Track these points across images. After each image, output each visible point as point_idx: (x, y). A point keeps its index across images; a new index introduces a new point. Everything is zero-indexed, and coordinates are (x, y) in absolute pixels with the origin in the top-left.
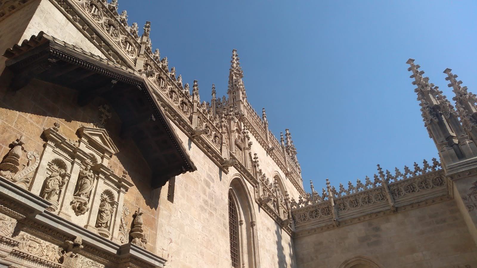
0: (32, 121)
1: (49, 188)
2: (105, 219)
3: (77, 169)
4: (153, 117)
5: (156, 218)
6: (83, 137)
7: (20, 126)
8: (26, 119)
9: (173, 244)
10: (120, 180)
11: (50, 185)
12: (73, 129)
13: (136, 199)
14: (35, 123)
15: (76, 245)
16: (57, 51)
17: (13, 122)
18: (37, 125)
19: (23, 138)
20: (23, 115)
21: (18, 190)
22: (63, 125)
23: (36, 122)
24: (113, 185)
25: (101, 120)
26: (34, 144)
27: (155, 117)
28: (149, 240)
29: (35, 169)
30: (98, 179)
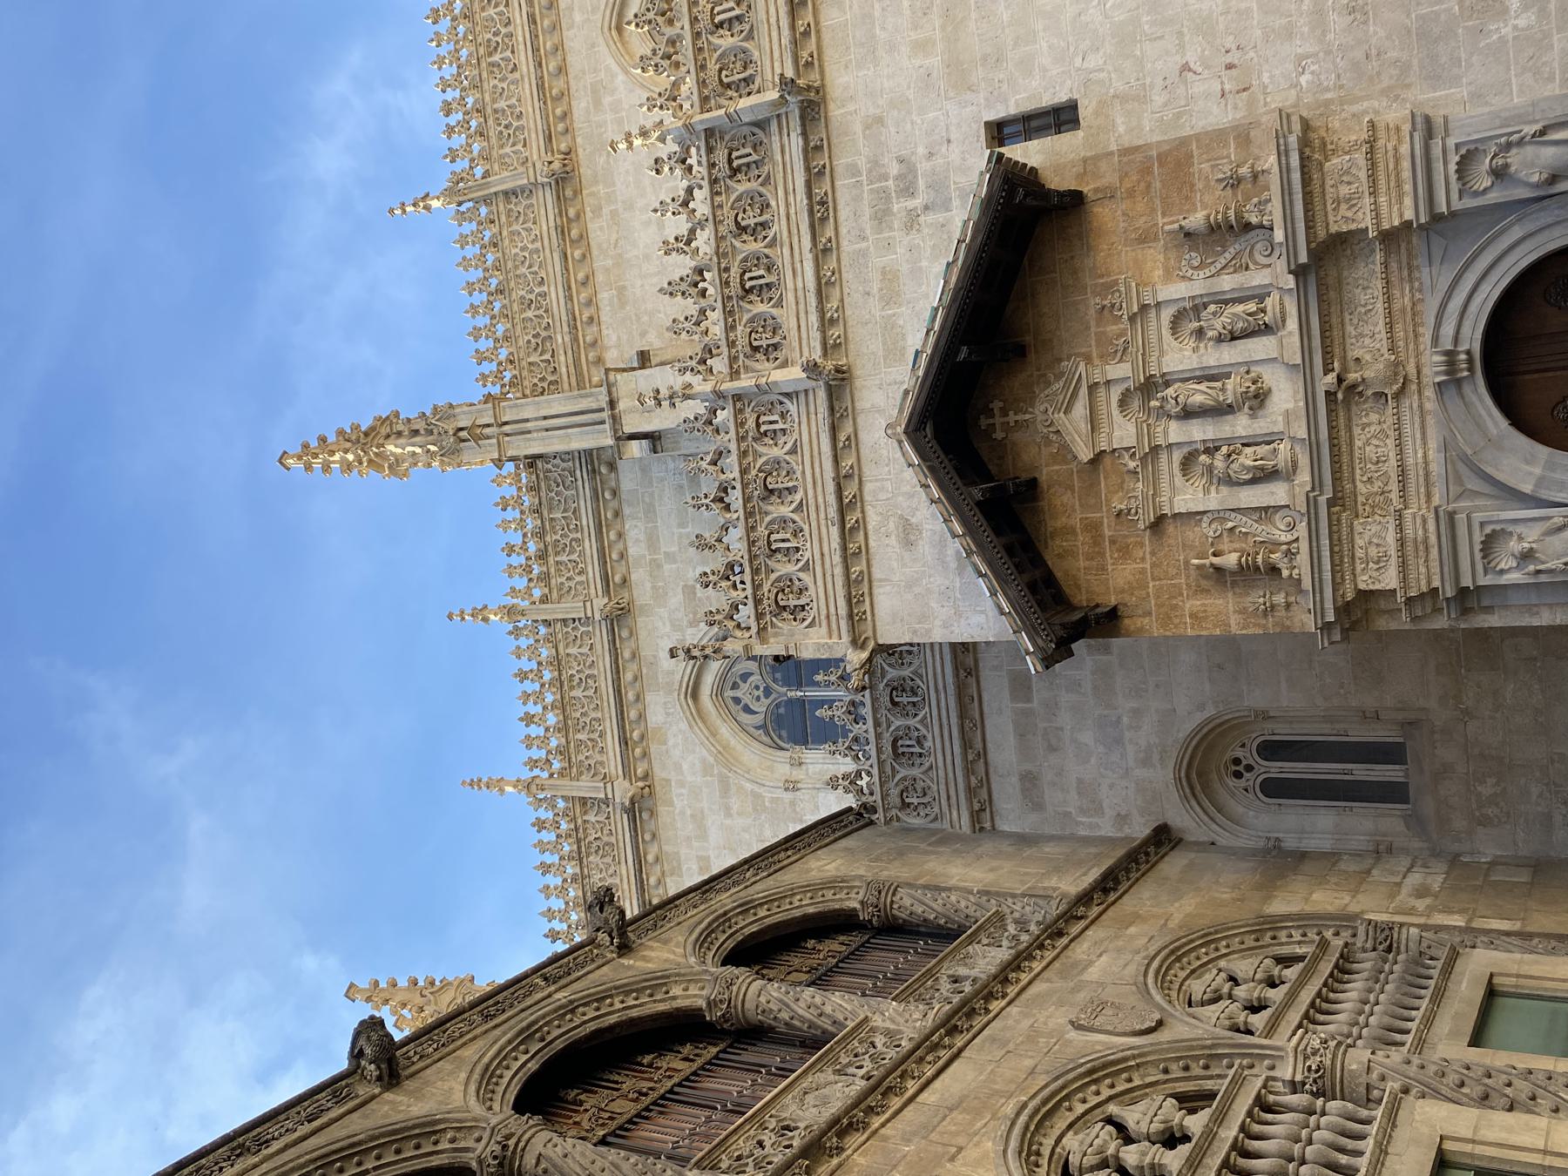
3: (1175, 432)
4: (961, 357)
5: (1155, 153)
9: (1191, 57)
10: (1132, 319)
15: (1340, 380)
19: (1196, 561)
24: (1153, 324)
27: (958, 352)
29: (1233, 515)
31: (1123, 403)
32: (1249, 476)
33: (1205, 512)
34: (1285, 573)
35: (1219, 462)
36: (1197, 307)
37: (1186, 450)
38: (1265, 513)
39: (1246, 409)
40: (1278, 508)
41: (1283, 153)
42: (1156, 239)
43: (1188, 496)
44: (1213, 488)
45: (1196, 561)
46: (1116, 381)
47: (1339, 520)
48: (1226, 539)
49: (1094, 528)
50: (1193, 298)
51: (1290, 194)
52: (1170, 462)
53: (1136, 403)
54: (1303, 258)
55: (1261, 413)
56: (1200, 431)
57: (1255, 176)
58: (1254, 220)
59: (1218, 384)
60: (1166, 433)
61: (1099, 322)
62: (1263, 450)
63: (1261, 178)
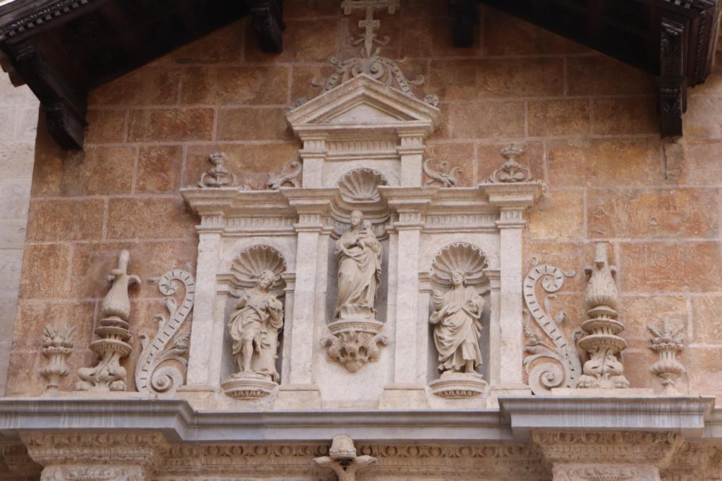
0: (146, 196)
1: (237, 342)
2: (449, 344)
6: (308, 141)
7: (119, 230)
8: (129, 200)
10: (482, 194)
11: (237, 333)
12: (271, 139)
13: (590, 218)
14: (155, 197)
15: (346, 462)
16: (14, 25)
17: (101, 228)
18: (165, 196)
19: (125, 256)
20: (121, 197)
21: (86, 408)
22: (239, 146)
23: (159, 189)
25: (363, 42)
26: (171, 250)
28: (694, 331)
29: (186, 312)
30: (396, 232)
31: (370, 178)
32: (236, 337)
33: (195, 275)
34: (87, 372)
35: (258, 299)
36: (485, 281)
37: (287, 256)
38: (180, 354)
39: (330, 336)
40: (184, 369)
41: (678, 407)
42: (592, 233)
43: (217, 252)
44: (225, 288)
45: (125, 256)
46: (398, 170)
47: (143, 444)
48: (152, 300)
49: (197, 126)
50: (498, 278)
51: (613, 412)
52: (273, 234)
53: (367, 194)
54: (518, 422)
55: (322, 357)
56: (308, 274)
57: (659, 374)
58: (589, 365)
59: (370, 304)
60: (311, 230)
61: (488, 151)
62: (268, 356)
63: (657, 382)
